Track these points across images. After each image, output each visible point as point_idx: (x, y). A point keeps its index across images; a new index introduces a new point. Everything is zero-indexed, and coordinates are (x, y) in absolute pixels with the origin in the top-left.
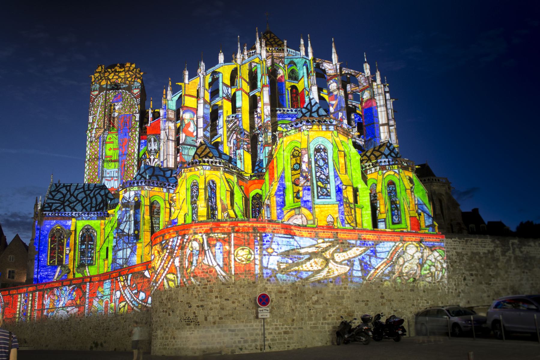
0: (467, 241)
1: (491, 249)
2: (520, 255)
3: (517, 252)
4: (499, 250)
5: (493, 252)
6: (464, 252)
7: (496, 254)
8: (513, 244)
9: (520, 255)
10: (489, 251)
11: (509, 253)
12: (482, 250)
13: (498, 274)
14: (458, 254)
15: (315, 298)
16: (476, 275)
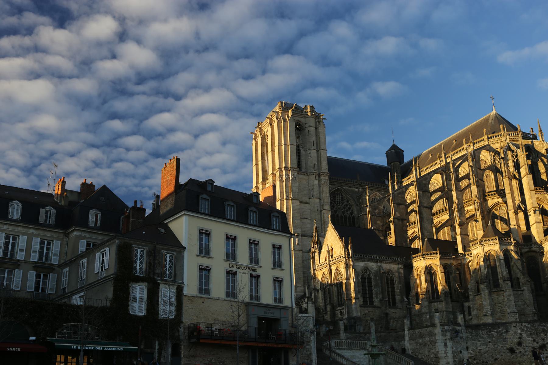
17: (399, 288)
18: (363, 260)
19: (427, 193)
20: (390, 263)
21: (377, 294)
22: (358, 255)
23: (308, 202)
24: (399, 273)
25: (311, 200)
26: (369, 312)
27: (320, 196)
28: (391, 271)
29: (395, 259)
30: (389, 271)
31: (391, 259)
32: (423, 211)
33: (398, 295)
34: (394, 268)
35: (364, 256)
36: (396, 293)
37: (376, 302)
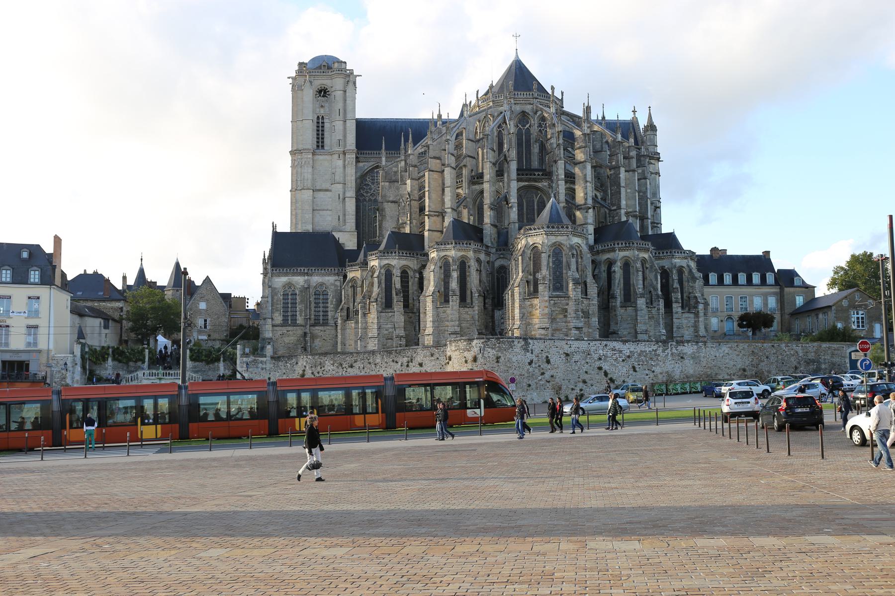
0: (638, 344)
1: (655, 349)
2: (676, 352)
3: (674, 350)
4: (660, 351)
5: (656, 351)
6: (635, 351)
7: (658, 352)
8: (671, 345)
9: (676, 352)
10: (653, 350)
11: (669, 351)
12: (648, 349)
13: (657, 364)
14: (631, 352)
15: (540, 378)
16: (642, 365)
17: (334, 303)
18: (286, 274)
19: (396, 183)
20: (324, 275)
21: (301, 311)
22: (280, 270)
23: (330, 188)
24: (336, 286)
25: (333, 186)
26: (288, 331)
27: (345, 181)
28: (325, 284)
29: (331, 270)
30: (322, 284)
31: (325, 270)
32: (386, 207)
33: (331, 311)
34: (328, 280)
35: (287, 270)
36: (329, 309)
37: (300, 320)
